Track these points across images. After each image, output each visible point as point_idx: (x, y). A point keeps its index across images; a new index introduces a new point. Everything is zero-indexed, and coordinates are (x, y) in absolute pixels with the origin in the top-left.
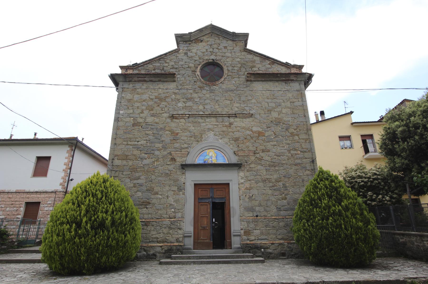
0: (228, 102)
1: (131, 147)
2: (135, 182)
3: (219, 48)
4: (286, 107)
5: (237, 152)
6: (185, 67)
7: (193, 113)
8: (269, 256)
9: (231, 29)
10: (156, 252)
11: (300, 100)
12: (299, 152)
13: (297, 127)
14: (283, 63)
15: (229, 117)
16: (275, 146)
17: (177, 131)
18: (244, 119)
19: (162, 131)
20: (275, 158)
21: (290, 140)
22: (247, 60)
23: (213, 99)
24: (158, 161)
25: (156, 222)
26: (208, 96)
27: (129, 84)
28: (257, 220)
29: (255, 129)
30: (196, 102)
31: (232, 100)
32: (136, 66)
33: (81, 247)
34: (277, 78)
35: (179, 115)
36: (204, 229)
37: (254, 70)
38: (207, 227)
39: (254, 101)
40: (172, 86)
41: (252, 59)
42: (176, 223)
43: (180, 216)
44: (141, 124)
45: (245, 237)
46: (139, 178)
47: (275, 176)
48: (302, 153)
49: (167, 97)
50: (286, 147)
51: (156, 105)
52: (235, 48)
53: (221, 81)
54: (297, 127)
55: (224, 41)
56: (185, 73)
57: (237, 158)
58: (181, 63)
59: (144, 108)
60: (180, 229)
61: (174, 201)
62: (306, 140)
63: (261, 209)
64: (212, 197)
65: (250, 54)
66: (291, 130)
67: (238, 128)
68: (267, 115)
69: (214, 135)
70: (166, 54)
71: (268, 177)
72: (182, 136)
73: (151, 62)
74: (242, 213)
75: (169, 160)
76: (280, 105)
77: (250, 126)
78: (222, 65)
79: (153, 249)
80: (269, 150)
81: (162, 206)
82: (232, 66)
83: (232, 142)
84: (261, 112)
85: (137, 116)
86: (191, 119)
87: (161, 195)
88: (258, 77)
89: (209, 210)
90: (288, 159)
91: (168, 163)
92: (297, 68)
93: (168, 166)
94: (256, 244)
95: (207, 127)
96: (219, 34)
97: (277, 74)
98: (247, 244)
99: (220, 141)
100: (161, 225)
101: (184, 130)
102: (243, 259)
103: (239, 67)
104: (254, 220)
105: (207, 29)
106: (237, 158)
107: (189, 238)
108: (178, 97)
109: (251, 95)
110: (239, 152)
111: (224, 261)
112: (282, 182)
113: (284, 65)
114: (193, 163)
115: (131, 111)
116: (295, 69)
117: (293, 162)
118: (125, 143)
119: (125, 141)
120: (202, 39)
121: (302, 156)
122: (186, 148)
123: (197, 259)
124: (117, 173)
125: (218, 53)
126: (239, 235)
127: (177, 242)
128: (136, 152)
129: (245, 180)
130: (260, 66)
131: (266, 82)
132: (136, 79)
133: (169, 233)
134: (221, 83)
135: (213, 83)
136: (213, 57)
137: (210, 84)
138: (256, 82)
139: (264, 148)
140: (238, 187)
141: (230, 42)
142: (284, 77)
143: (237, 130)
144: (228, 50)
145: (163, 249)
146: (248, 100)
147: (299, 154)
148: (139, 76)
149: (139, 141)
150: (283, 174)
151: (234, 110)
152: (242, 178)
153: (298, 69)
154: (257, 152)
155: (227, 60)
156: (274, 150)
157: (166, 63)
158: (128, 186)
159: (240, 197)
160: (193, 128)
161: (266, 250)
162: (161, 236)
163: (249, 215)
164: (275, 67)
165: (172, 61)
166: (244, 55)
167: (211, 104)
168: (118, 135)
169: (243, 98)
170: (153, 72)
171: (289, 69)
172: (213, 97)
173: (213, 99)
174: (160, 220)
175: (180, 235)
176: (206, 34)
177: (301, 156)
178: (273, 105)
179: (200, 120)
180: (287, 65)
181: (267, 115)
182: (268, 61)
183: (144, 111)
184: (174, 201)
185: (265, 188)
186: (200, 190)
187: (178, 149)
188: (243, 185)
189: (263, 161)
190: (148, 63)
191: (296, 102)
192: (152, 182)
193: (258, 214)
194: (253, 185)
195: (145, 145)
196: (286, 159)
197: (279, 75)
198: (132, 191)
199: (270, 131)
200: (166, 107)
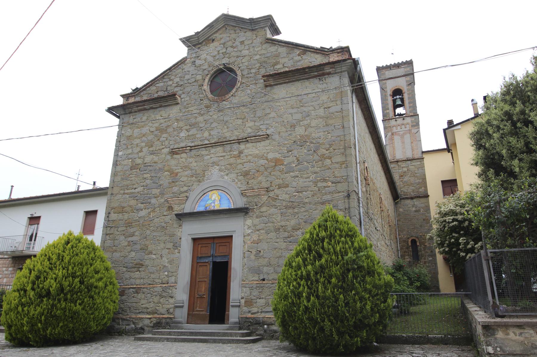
0: (240, 122)
1: (128, 196)
2: (130, 239)
3: (234, 45)
4: (318, 117)
5: (244, 192)
6: (191, 82)
7: (196, 144)
8: (273, 336)
9: (247, 15)
10: (145, 325)
11: (339, 102)
12: (330, 184)
13: (331, 145)
14: (317, 49)
15: (239, 143)
16: (297, 178)
17: (177, 171)
18: (258, 144)
19: (161, 173)
20: (295, 196)
21: (318, 166)
22: (268, 55)
23: (221, 121)
24: (154, 212)
25: (147, 288)
26: (215, 117)
27: (130, 117)
28: (262, 285)
29: (271, 156)
30: (201, 127)
31: (245, 118)
32: (137, 91)
33: (24, 317)
34: (306, 75)
35: (179, 148)
36: (201, 297)
37: (276, 68)
38: (204, 295)
39: (273, 115)
40: (173, 112)
41: (275, 53)
42: (168, 290)
43: (173, 281)
44: (140, 166)
45: (245, 309)
46: (133, 235)
47: (293, 222)
48: (334, 185)
49: (169, 126)
50: (312, 177)
51: (156, 139)
52: (255, 41)
53: (232, 94)
54: (331, 145)
55: (242, 34)
56: (191, 91)
57: (245, 199)
58: (187, 77)
59: (143, 144)
60: (172, 297)
61: (168, 262)
62: (343, 163)
63: (270, 270)
64: (213, 256)
65: (274, 45)
66: (322, 151)
67: (250, 157)
68: (289, 133)
69: (219, 171)
70: (170, 69)
71: (283, 223)
72: (182, 176)
73: (154, 82)
74: (246, 275)
75: (166, 208)
76: (309, 116)
77: (265, 153)
78: (235, 69)
79: (142, 322)
80: (287, 185)
81: (156, 268)
82: (249, 69)
83: (241, 178)
84: (281, 130)
85: (136, 156)
86: (194, 152)
87: (155, 255)
88: (279, 79)
89: (208, 272)
90: (313, 196)
91: (165, 214)
92: (338, 53)
93: (165, 217)
94: (258, 318)
95: (212, 160)
96: (235, 25)
97: (304, 69)
98: (247, 318)
99: (226, 177)
100: (152, 292)
101: (186, 167)
102: (230, 338)
103: (258, 68)
104: (258, 285)
105: (218, 21)
106: (244, 200)
107: (181, 309)
108: (181, 124)
109: (270, 106)
110: (247, 191)
111: (200, 339)
112: (301, 231)
113: (319, 52)
114: (191, 211)
115: (130, 151)
116: (335, 55)
117: (319, 199)
118: (122, 192)
119: (122, 190)
120: (213, 38)
121: (334, 189)
122: (186, 192)
123: (178, 335)
124: (112, 229)
125: (232, 53)
126: (239, 306)
127: (168, 313)
128: (133, 202)
129: (252, 229)
130: (286, 60)
131: (291, 84)
132: (136, 109)
133: (160, 303)
134: (233, 95)
135: (222, 98)
136: (225, 61)
137: (218, 101)
138: (278, 86)
139: (281, 182)
140: (242, 240)
141: (249, 34)
142: (315, 72)
143: (248, 161)
144: (245, 45)
145: (151, 322)
146: (266, 115)
147: (329, 187)
148: (137, 104)
149: (136, 188)
150: (304, 218)
151: (246, 132)
152: (249, 227)
153: (341, 54)
154: (271, 188)
155: (243, 61)
156: (294, 184)
157: (170, 80)
158: (122, 245)
159: (244, 253)
160: (195, 164)
161: (270, 326)
162: (151, 306)
163: (253, 279)
164: (306, 57)
165: (177, 76)
166: (266, 49)
167: (218, 127)
168: (116, 183)
169: (259, 114)
170: (156, 96)
171: (327, 57)
172: (221, 118)
173: (221, 121)
174: (151, 286)
175: (171, 305)
176: (219, 30)
177: (332, 189)
178: (298, 116)
179: (204, 152)
180: (322, 51)
181: (289, 133)
182: (297, 50)
183: (143, 149)
184: (168, 262)
185: (278, 240)
186: (200, 246)
187: (176, 195)
188: (250, 237)
189: (278, 201)
190: (151, 85)
191: (332, 106)
192: (146, 238)
193: (265, 277)
194: (262, 237)
195: (142, 193)
196: (311, 196)
197: (306, 70)
198: (126, 251)
199: (291, 156)
200: (167, 140)
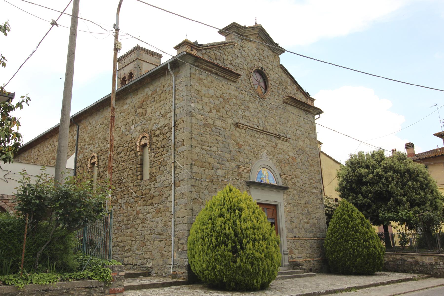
1: (205, 152)
14: (304, 92)
15: (275, 137)
119: (199, 144)
128: (210, 160)
132: (204, 66)
156: (302, 178)
160: (252, 142)
